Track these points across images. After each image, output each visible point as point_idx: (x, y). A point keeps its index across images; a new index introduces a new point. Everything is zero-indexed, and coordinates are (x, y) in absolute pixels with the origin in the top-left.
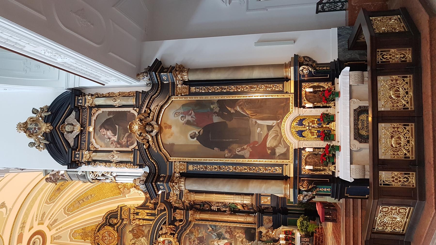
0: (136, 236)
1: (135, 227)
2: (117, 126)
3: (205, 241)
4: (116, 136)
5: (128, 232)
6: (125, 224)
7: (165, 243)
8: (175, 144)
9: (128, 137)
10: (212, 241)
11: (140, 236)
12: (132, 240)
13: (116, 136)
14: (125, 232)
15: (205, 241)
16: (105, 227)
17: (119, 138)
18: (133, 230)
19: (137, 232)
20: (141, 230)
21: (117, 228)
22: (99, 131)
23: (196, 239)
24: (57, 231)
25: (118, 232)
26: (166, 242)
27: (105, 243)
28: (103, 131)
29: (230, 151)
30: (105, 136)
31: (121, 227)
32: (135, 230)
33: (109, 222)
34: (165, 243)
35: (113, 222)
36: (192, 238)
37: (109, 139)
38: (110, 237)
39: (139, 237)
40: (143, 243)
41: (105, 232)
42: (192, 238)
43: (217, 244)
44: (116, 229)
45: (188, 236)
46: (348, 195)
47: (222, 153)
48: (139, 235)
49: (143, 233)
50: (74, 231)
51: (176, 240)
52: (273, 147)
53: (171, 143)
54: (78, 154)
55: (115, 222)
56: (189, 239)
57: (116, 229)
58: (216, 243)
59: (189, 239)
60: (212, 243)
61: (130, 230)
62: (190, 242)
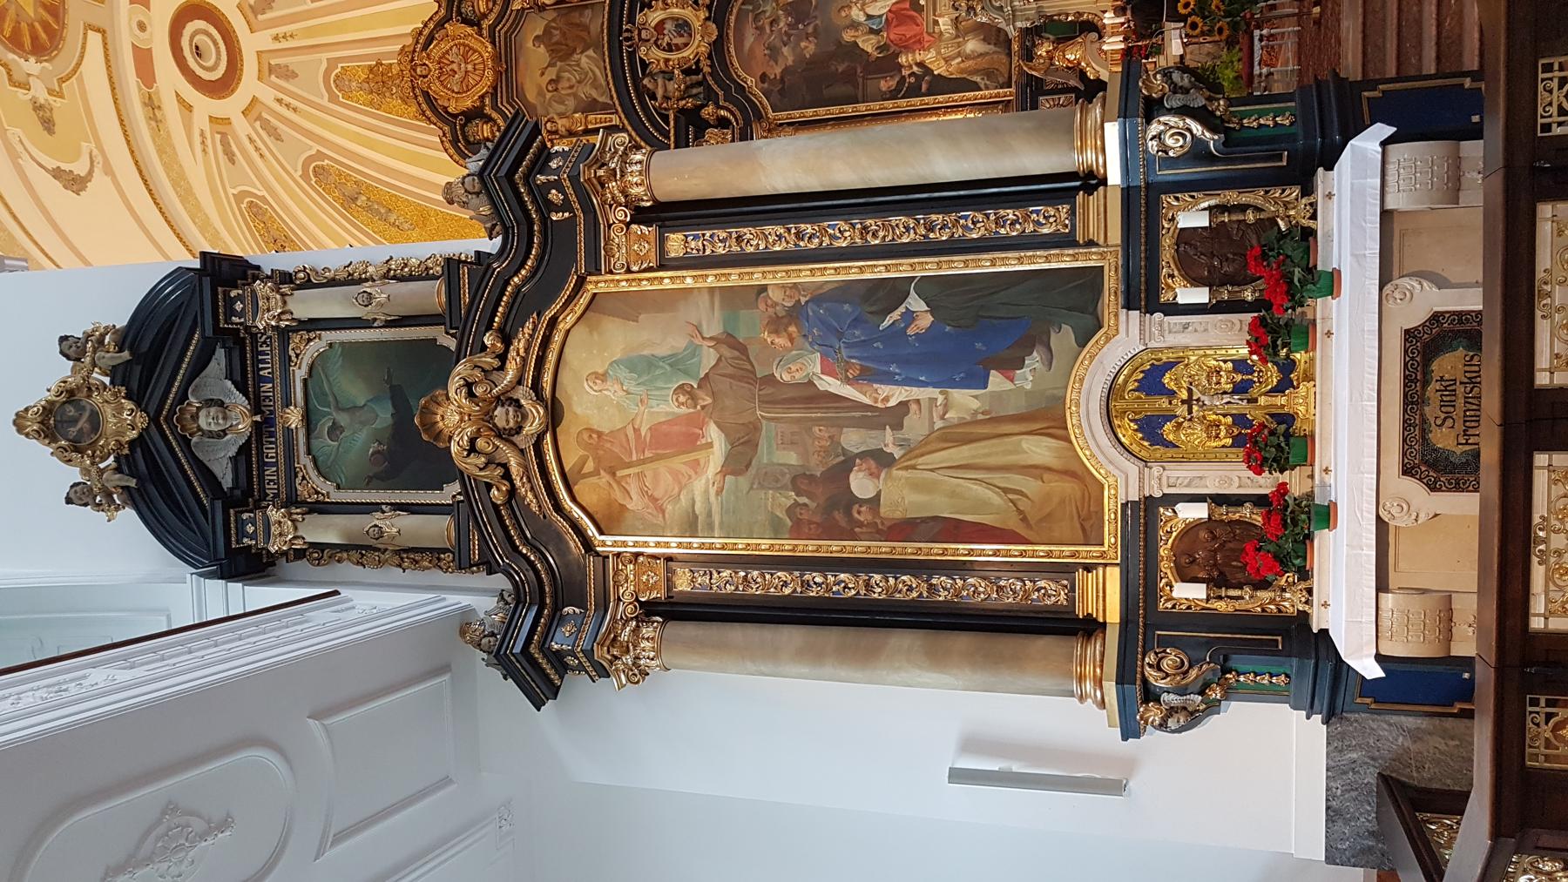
0: (561, 52)
1: (554, 20)
3: (816, 13)
5: (530, 44)
6: (518, 10)
7: (666, 32)
10: (843, 7)
11: (574, 50)
12: (546, 68)
14: (521, 47)
15: (816, 13)
16: (446, 25)
18: (547, 31)
19: (564, 34)
20: (578, 25)
21: (492, 28)
23: (781, 12)
24: (278, 46)
25: (493, 43)
26: (669, 26)
27: (453, 91)
31: (501, 29)
32: (555, 28)
33: (459, 13)
34: (666, 32)
35: (473, 7)
36: (764, 12)
38: (466, 63)
39: (571, 54)
40: (587, 74)
41: (447, 52)
42: (764, 12)
43: (862, 13)
44: (485, 32)
45: (751, 8)
48: (569, 42)
49: (584, 34)
50: (339, 70)
51: (703, 14)
55: (482, 10)
56: (756, 18)
57: (485, 32)
58: (857, 12)
59: (756, 18)
60: (843, 14)
61: (539, 32)
62: (760, 29)
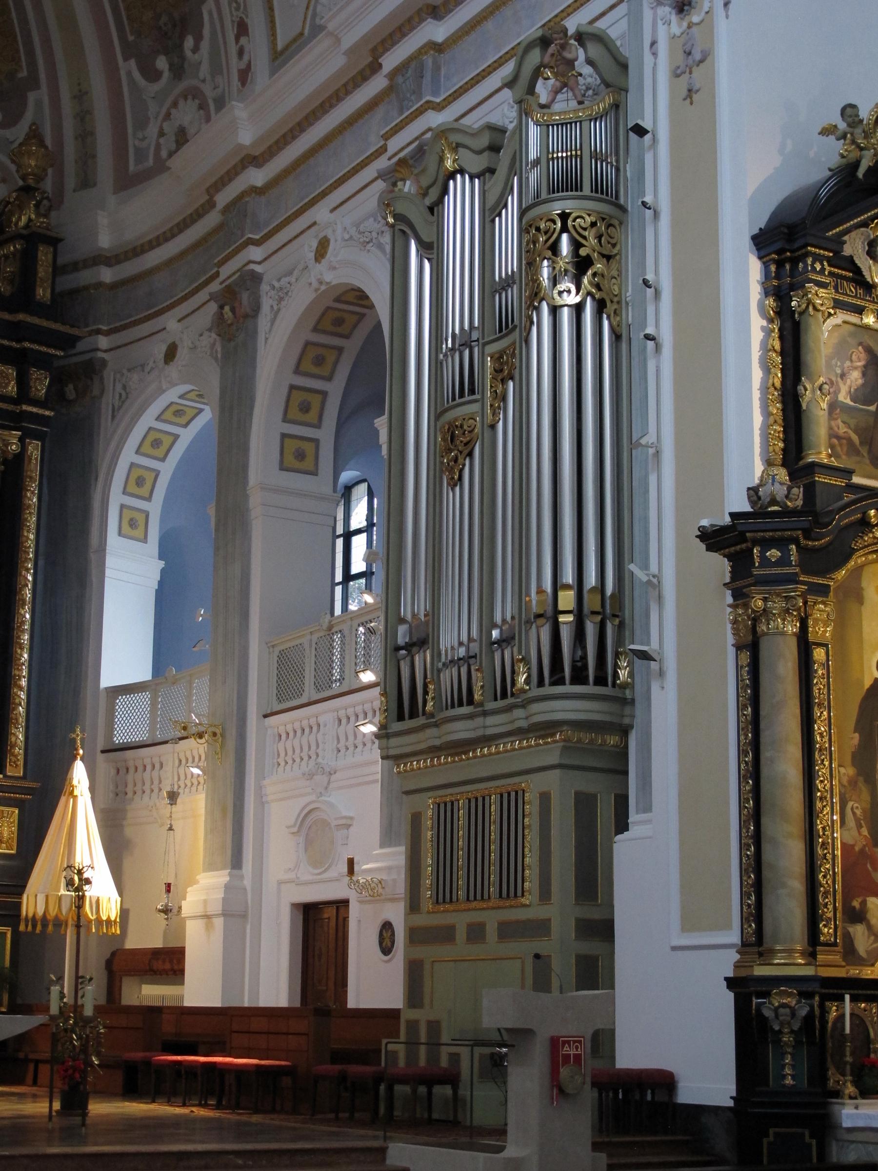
2: (873, 408)
4: (848, 401)
8: (863, 608)
9: (850, 441)
13: (848, 401)
17: (845, 408)
22: (860, 344)
28: (860, 359)
29: (853, 783)
30: (848, 363)
37: (843, 376)
46: (771, 1138)
47: (848, 758)
52: (869, 916)
53: (865, 593)
54: (823, 269)
